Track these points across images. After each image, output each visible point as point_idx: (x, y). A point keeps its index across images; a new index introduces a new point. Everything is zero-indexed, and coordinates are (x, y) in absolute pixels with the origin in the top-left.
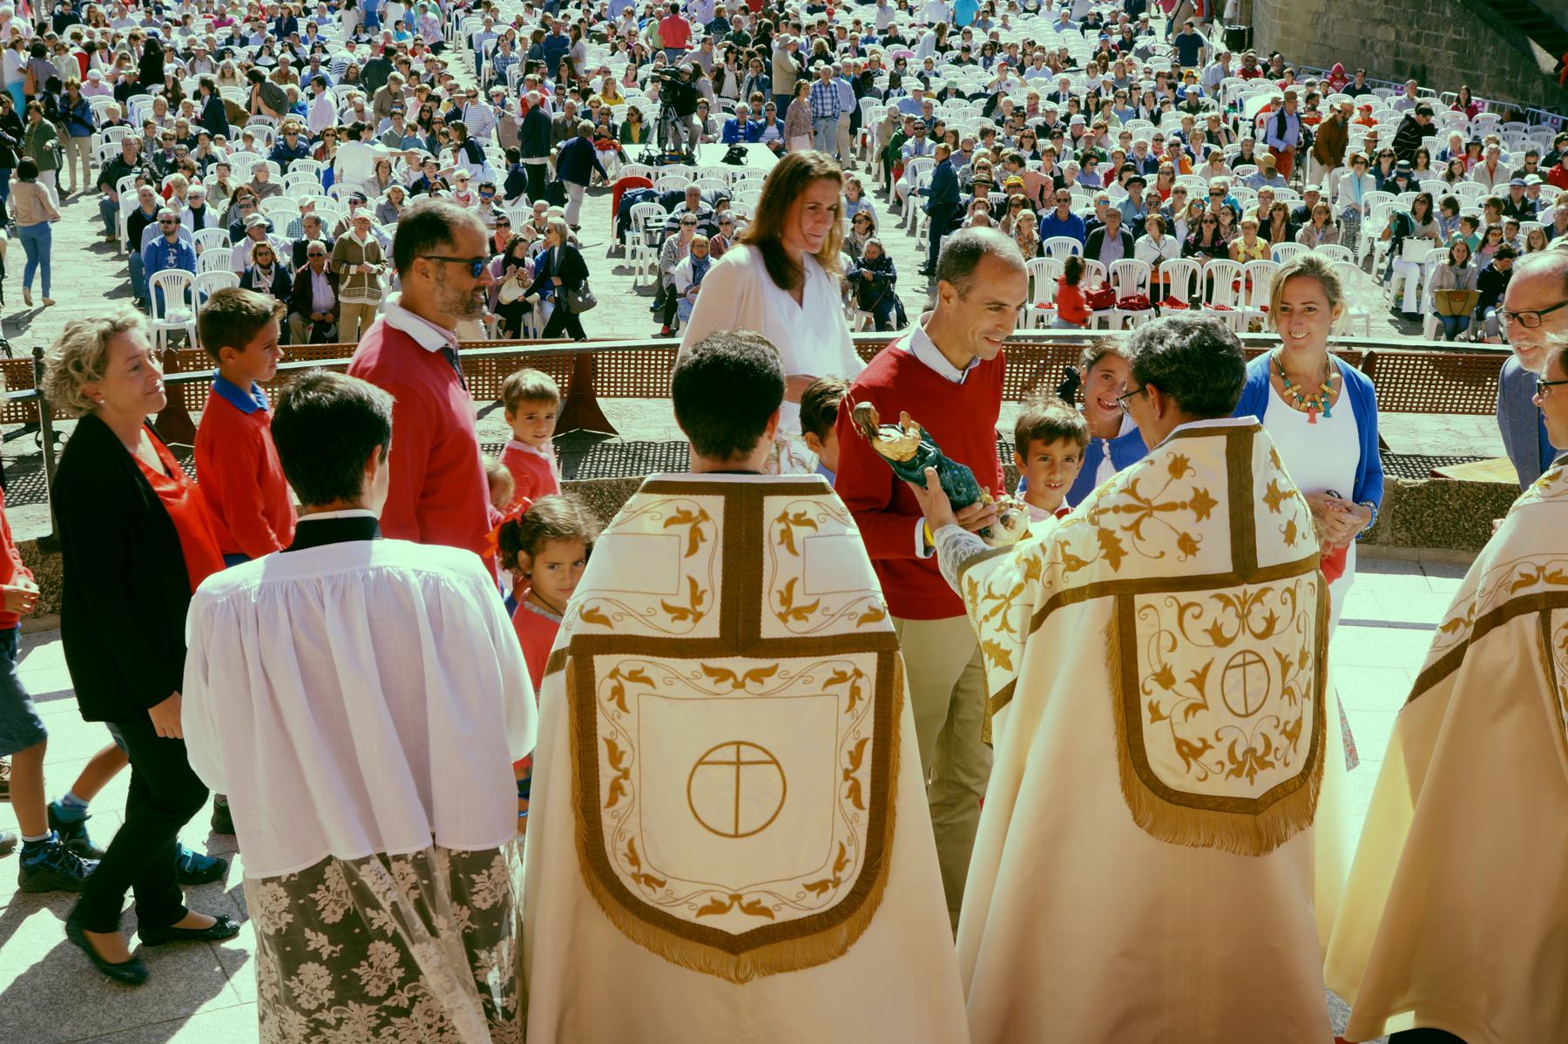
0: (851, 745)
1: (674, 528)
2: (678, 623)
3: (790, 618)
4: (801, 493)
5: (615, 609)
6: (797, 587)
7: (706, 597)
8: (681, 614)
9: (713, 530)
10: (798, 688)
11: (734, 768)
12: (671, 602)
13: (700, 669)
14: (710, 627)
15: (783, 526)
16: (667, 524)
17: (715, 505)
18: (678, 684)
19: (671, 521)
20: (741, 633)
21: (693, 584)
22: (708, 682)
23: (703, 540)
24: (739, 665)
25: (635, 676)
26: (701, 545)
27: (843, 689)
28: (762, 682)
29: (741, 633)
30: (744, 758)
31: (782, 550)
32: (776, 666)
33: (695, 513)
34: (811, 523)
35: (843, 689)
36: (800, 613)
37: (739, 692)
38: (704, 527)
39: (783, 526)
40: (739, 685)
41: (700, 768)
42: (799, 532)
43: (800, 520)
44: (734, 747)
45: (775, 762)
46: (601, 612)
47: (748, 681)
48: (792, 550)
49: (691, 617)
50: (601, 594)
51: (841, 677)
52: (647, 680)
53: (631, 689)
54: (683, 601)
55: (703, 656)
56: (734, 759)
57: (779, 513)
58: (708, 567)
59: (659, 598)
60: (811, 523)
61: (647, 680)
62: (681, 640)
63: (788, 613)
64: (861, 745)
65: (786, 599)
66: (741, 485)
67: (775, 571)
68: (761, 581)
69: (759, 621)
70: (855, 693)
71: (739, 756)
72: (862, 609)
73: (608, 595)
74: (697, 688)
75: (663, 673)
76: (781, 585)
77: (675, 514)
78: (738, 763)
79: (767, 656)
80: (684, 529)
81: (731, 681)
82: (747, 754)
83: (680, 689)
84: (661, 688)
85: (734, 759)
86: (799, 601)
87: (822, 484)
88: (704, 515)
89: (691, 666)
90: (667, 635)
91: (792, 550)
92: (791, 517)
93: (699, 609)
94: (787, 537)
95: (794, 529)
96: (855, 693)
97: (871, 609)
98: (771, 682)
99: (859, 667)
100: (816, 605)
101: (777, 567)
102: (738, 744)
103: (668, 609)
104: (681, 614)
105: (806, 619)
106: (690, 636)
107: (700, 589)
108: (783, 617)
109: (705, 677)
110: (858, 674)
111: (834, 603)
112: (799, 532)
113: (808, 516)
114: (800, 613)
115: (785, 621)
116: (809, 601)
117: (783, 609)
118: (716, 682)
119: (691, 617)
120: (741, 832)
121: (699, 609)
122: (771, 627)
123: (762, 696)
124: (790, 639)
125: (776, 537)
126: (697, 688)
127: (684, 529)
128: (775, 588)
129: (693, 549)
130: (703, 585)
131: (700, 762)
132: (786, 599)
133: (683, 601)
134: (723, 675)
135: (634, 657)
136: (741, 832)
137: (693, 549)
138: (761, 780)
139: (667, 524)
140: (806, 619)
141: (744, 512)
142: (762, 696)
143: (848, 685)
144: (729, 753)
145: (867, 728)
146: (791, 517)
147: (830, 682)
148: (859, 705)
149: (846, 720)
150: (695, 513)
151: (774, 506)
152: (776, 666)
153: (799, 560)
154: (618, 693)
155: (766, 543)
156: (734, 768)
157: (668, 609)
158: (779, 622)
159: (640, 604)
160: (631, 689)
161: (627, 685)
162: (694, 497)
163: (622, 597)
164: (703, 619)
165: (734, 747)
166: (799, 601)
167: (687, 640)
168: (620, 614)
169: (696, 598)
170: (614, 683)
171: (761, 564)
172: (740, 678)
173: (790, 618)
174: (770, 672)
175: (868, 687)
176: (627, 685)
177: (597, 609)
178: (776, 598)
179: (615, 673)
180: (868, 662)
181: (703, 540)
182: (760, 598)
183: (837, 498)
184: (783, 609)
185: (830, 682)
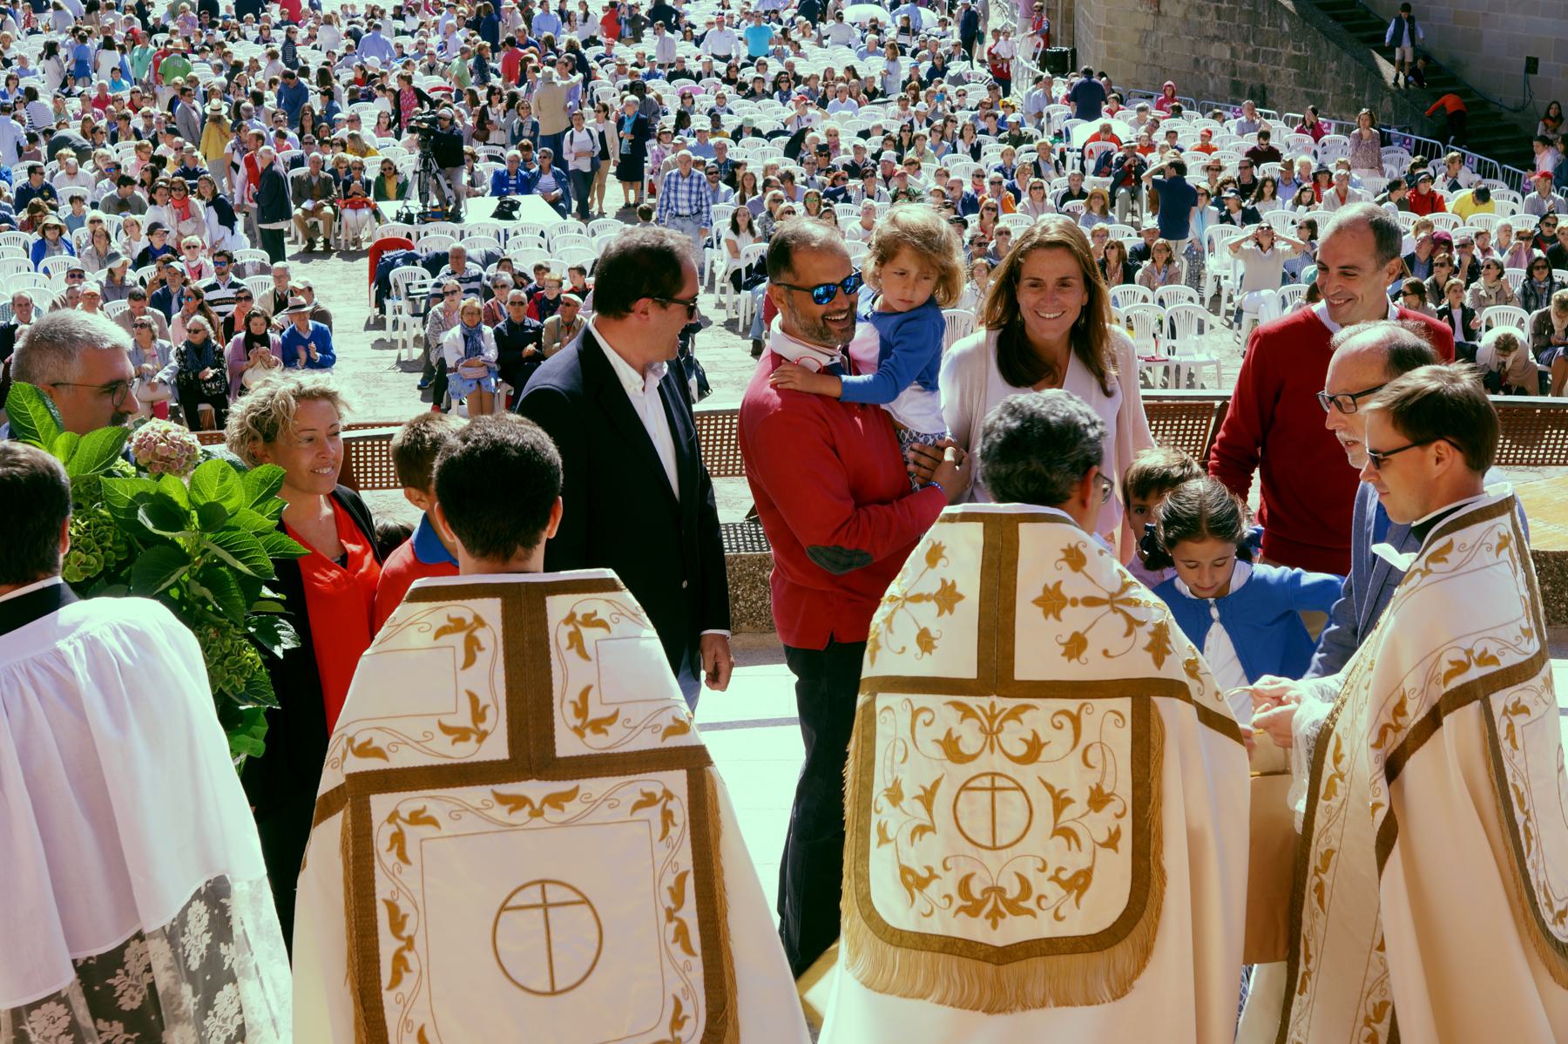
0: (670, 880)
1: (446, 639)
2: (460, 745)
3: (588, 732)
4: (590, 591)
5: (390, 739)
6: (593, 697)
7: (490, 713)
8: (461, 734)
9: (492, 636)
10: (604, 813)
11: (540, 912)
12: (450, 721)
14: (496, 748)
15: (571, 628)
16: (438, 634)
17: (491, 609)
18: (468, 817)
19: (441, 632)
20: (532, 752)
21: (474, 699)
22: (500, 812)
23: (480, 649)
24: (535, 789)
25: (417, 818)
26: (479, 654)
27: (654, 813)
28: (562, 808)
29: (532, 752)
30: (551, 898)
31: (572, 656)
32: (577, 789)
33: (469, 620)
34: (602, 624)
35: (654, 813)
36: (598, 726)
37: (538, 822)
38: (480, 634)
39: (571, 628)
40: (537, 813)
41: (504, 914)
42: (590, 635)
43: (591, 621)
44: (538, 888)
45: (586, 901)
46: (375, 744)
47: (546, 808)
49: (474, 737)
51: (649, 800)
52: (432, 821)
53: (413, 834)
54: (464, 719)
55: (492, 782)
56: (540, 901)
57: (565, 614)
58: (489, 677)
59: (435, 719)
60: (602, 624)
61: (432, 821)
62: (465, 765)
63: (584, 726)
64: (681, 879)
65: (581, 710)
66: (519, 584)
67: (566, 678)
68: (551, 691)
69: (553, 737)
70: (667, 816)
71: (545, 897)
72: (666, 721)
74: (491, 820)
75: (449, 807)
76: (574, 694)
77: (445, 622)
78: (545, 906)
79: (565, 779)
80: (458, 639)
81: (527, 809)
82: (554, 894)
83: (470, 822)
84: (447, 826)
85: (540, 901)
86: (595, 712)
87: (612, 580)
88: (479, 621)
89: (477, 795)
90: (448, 762)
92: (579, 618)
93: (482, 727)
94: (576, 640)
96: (667, 816)
97: (676, 720)
98: (572, 808)
99: (669, 787)
100: (616, 715)
102: (543, 882)
103: (446, 729)
104: (461, 734)
105: (605, 732)
106: (474, 759)
107: (482, 704)
108: (579, 731)
109: (497, 805)
110: (668, 795)
112: (590, 635)
113: (599, 616)
114: (598, 726)
115: (582, 735)
116: (607, 712)
117: (578, 722)
118: (511, 811)
119: (474, 737)
120: (558, 987)
121: (482, 727)
122: (567, 744)
123: (564, 824)
124: (589, 757)
127: (458, 639)
128: (568, 697)
129: (470, 660)
131: (503, 908)
132: (581, 710)
133: (464, 719)
134: (518, 802)
135: (414, 794)
136: (558, 987)
137: (470, 660)
138: (572, 925)
139: (438, 634)
140: (605, 732)
141: (524, 611)
143: (660, 806)
144: (533, 895)
145: (685, 860)
146: (579, 618)
147: (638, 806)
148: (674, 832)
149: (662, 852)
150: (469, 620)
151: (558, 607)
152: (577, 789)
153: (592, 665)
154: (398, 840)
156: (540, 912)
157: (446, 729)
158: (576, 737)
159: (414, 729)
160: (413, 834)
161: (407, 828)
162: (466, 602)
164: (488, 739)
165: (538, 888)
166: (595, 712)
167: (472, 764)
168: (393, 744)
169: (478, 715)
170: (392, 829)
171: (549, 672)
172: (537, 805)
173: (588, 732)
174: (572, 795)
175: (680, 809)
176: (407, 828)
178: (569, 710)
179: (393, 817)
180: (677, 780)
181: (480, 649)
182: (552, 711)
183: (630, 596)
184: (578, 722)
185: (638, 806)
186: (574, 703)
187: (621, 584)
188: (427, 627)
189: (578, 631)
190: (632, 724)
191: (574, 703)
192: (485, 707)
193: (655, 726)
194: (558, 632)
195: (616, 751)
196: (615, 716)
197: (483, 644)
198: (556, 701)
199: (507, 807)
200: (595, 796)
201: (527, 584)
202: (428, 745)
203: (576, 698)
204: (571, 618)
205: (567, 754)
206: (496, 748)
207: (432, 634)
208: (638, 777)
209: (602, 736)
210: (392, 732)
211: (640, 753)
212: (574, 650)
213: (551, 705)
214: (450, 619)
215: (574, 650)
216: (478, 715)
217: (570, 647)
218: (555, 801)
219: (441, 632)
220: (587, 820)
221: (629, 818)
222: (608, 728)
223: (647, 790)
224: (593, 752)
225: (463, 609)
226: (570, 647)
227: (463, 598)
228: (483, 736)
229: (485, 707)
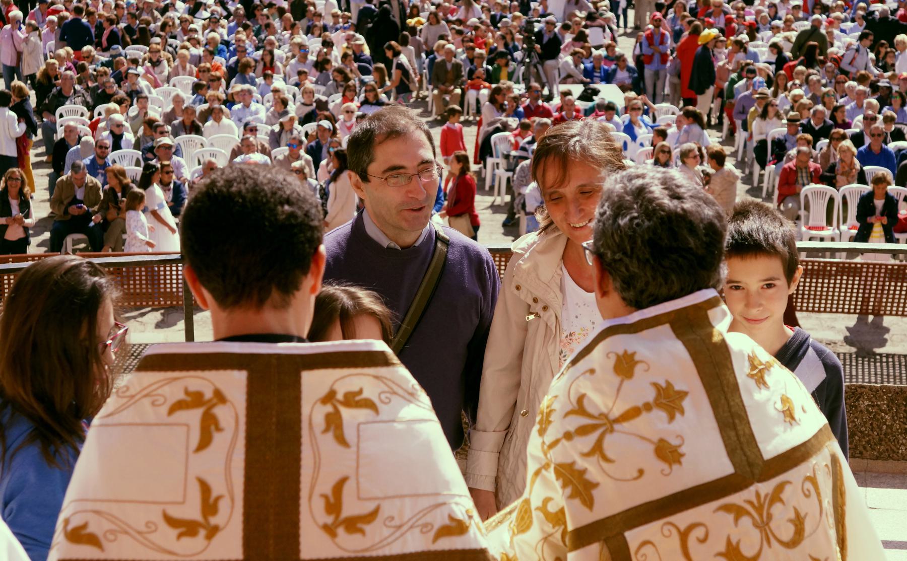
2: (186, 540)
3: (341, 531)
5: (107, 526)
6: (348, 491)
7: (224, 506)
9: (233, 415)
12: (176, 512)
15: (329, 408)
16: (173, 410)
17: (235, 383)
19: (179, 406)
21: (205, 488)
23: (219, 429)
26: (217, 438)
31: (327, 441)
33: (208, 394)
34: (369, 404)
36: (353, 525)
38: (220, 412)
39: (329, 408)
43: (353, 400)
46: (91, 529)
48: (341, 440)
49: (202, 533)
50: (90, 506)
54: (192, 511)
57: (324, 391)
58: (225, 464)
60: (369, 404)
63: (336, 524)
65: (334, 504)
67: (317, 467)
72: (439, 519)
73: (98, 506)
77: (181, 396)
80: (194, 416)
86: (350, 508)
87: (383, 354)
88: (220, 397)
91: (341, 440)
92: (340, 396)
93: (213, 521)
94: (334, 423)
95: (347, 414)
101: (319, 462)
103: (172, 522)
105: (363, 532)
107: (214, 494)
108: (330, 530)
113: (366, 394)
114: (353, 525)
117: (329, 520)
119: (202, 533)
121: (213, 521)
127: (194, 416)
128: (319, 490)
129: (205, 442)
130: (218, 488)
132: (334, 504)
133: (192, 511)
137: (205, 442)
139: (173, 410)
140: (363, 532)
146: (340, 396)
150: (208, 394)
151: (314, 383)
157: (172, 522)
158: (325, 537)
159: (137, 517)
162: (208, 374)
163: (114, 509)
164: (218, 538)
166: (350, 508)
168: (112, 532)
169: (209, 506)
173: (341, 531)
177: (85, 526)
178: (319, 505)
181: (219, 429)
183: (403, 371)
184: (329, 520)
186: (325, 497)
187: (395, 359)
188: (161, 400)
189: (337, 413)
190: (397, 522)
191: (325, 497)
192: (218, 498)
193: (425, 525)
194: (313, 412)
195: (374, 554)
196: (371, 516)
197: (223, 423)
201: (279, 357)
202: (148, 536)
203: (327, 489)
204: (330, 397)
205: (315, 556)
207: (164, 410)
209: (358, 536)
210: (111, 518)
212: (330, 436)
214: (187, 392)
215: (330, 436)
216: (209, 506)
217: (326, 430)
219: (179, 406)
222: (368, 528)
224: (346, 555)
225: (202, 381)
226: (326, 430)
227: (203, 368)
228: (213, 531)
229: (218, 498)
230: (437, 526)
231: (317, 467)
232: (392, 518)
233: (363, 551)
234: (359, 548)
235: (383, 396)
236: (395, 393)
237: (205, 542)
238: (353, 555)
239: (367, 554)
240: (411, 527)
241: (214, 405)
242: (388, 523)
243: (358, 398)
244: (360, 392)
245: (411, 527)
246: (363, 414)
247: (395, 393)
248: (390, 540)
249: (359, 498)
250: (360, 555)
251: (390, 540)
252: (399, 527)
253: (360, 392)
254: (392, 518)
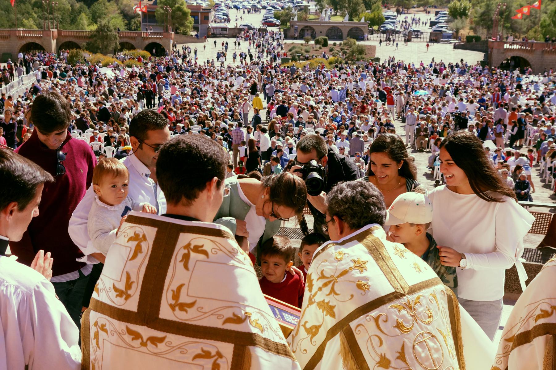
3: (177, 308)
6: (184, 291)
7: (134, 286)
9: (147, 247)
13: (125, 329)
21: (128, 277)
22: (128, 338)
24: (146, 332)
31: (180, 265)
36: (183, 307)
37: (143, 349)
40: (144, 344)
43: (198, 249)
47: (149, 343)
48: (186, 267)
60: (205, 253)
65: (176, 295)
66: (169, 223)
67: (173, 277)
72: (228, 314)
74: (123, 340)
76: (174, 287)
81: (140, 340)
86: (184, 299)
92: (192, 247)
93: (129, 292)
94: (186, 257)
95: (193, 254)
98: (161, 347)
99: (221, 350)
101: (176, 275)
105: (186, 311)
107: (132, 280)
108: (173, 307)
109: (127, 334)
111: (208, 306)
113: (204, 248)
114: (183, 307)
116: (189, 301)
117: (173, 302)
118: (133, 339)
122: (166, 313)
123: (156, 354)
125: (180, 257)
126: (123, 340)
129: (134, 256)
130: (133, 278)
132: (176, 295)
134: (136, 336)
137: (134, 256)
140: (186, 311)
142: (156, 354)
146: (192, 247)
151: (184, 239)
155: (173, 260)
158: (171, 310)
162: (143, 227)
166: (184, 299)
172: (145, 340)
173: (177, 308)
178: (170, 294)
190: (204, 310)
192: (133, 282)
193: (220, 315)
194: (179, 251)
195: (190, 323)
196: (192, 305)
197: (143, 250)
198: (165, 288)
199: (132, 337)
200: (174, 345)
203: (175, 288)
204: (188, 246)
206: (132, 305)
208: (202, 340)
209: (184, 313)
211: (206, 328)
212: (182, 263)
213: (162, 289)
217: (181, 261)
218: (154, 340)
220: (167, 356)
221: (191, 361)
223: (206, 349)
224: (177, 320)
226: (181, 261)
230: (226, 316)
231: (173, 277)
232: (202, 308)
233: (185, 320)
234: (184, 319)
235: (213, 250)
236: (221, 250)
237: (125, 301)
238: (180, 321)
239: (187, 322)
240: (212, 314)
241: (142, 241)
242: (199, 309)
243: (200, 249)
244: (202, 246)
245: (212, 314)
246: (202, 257)
247: (221, 250)
248: (198, 318)
249: (187, 295)
250: (184, 322)
251: (198, 318)
252: (206, 313)
253: (202, 246)
254: (202, 308)
